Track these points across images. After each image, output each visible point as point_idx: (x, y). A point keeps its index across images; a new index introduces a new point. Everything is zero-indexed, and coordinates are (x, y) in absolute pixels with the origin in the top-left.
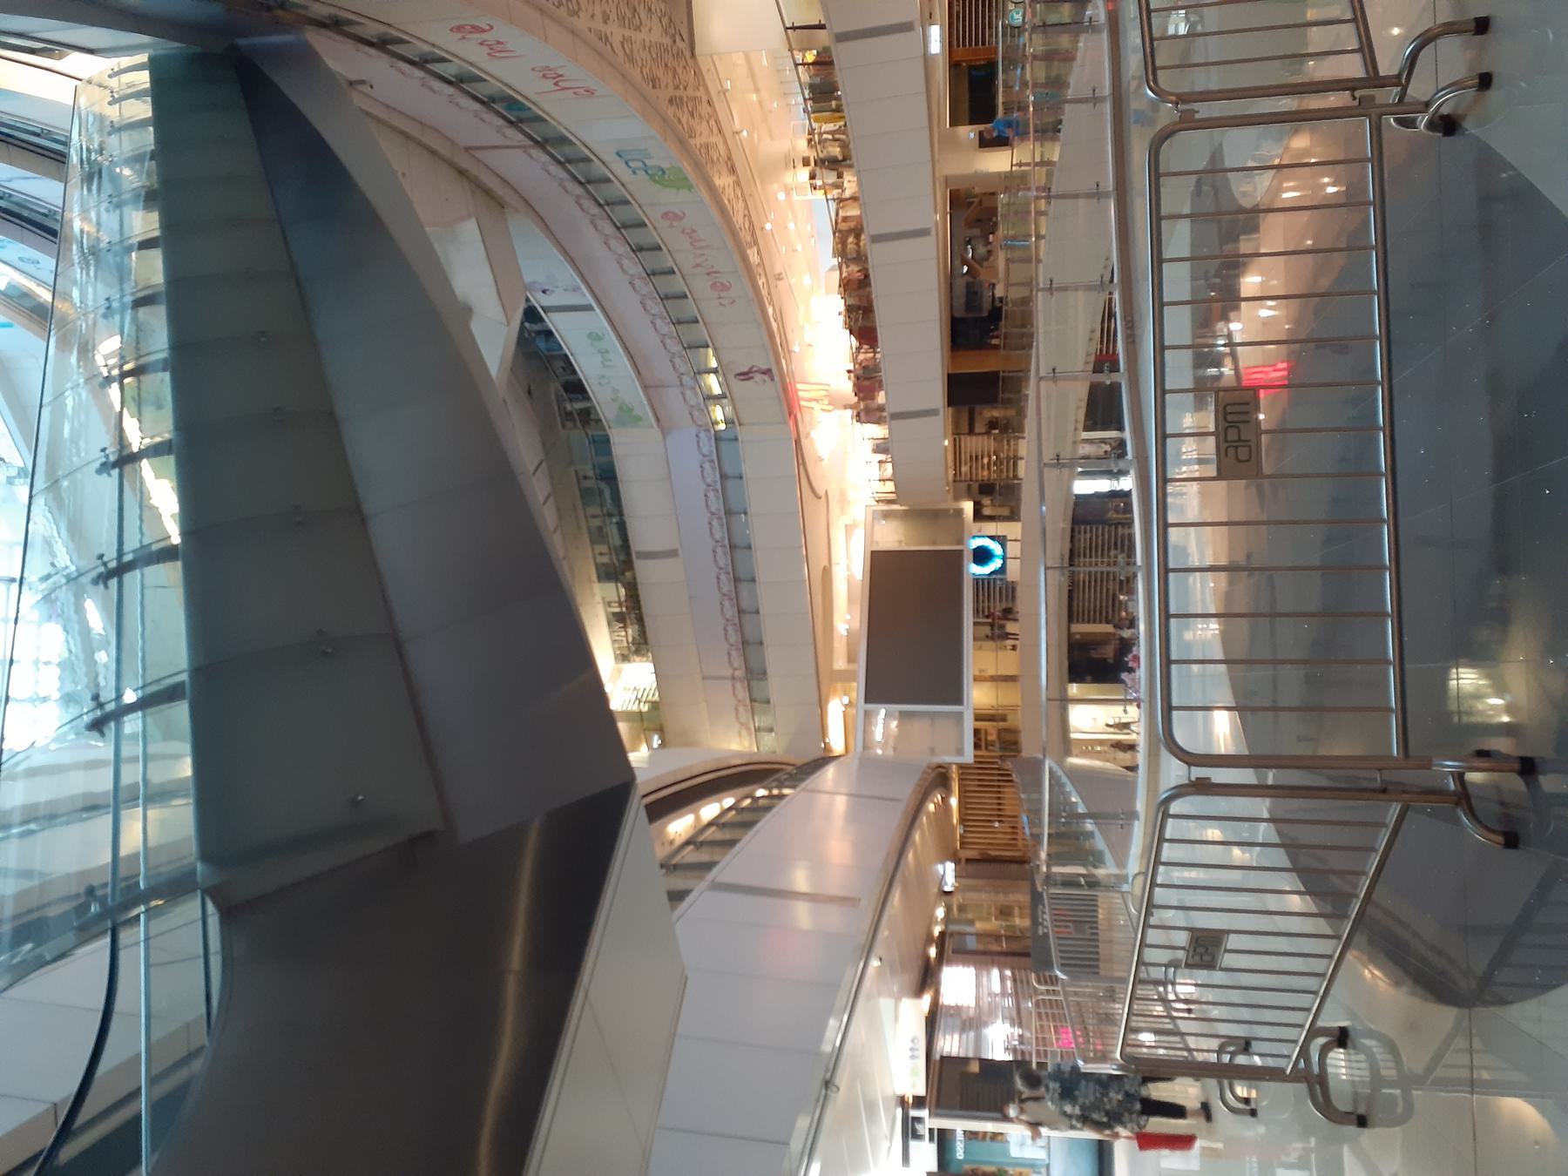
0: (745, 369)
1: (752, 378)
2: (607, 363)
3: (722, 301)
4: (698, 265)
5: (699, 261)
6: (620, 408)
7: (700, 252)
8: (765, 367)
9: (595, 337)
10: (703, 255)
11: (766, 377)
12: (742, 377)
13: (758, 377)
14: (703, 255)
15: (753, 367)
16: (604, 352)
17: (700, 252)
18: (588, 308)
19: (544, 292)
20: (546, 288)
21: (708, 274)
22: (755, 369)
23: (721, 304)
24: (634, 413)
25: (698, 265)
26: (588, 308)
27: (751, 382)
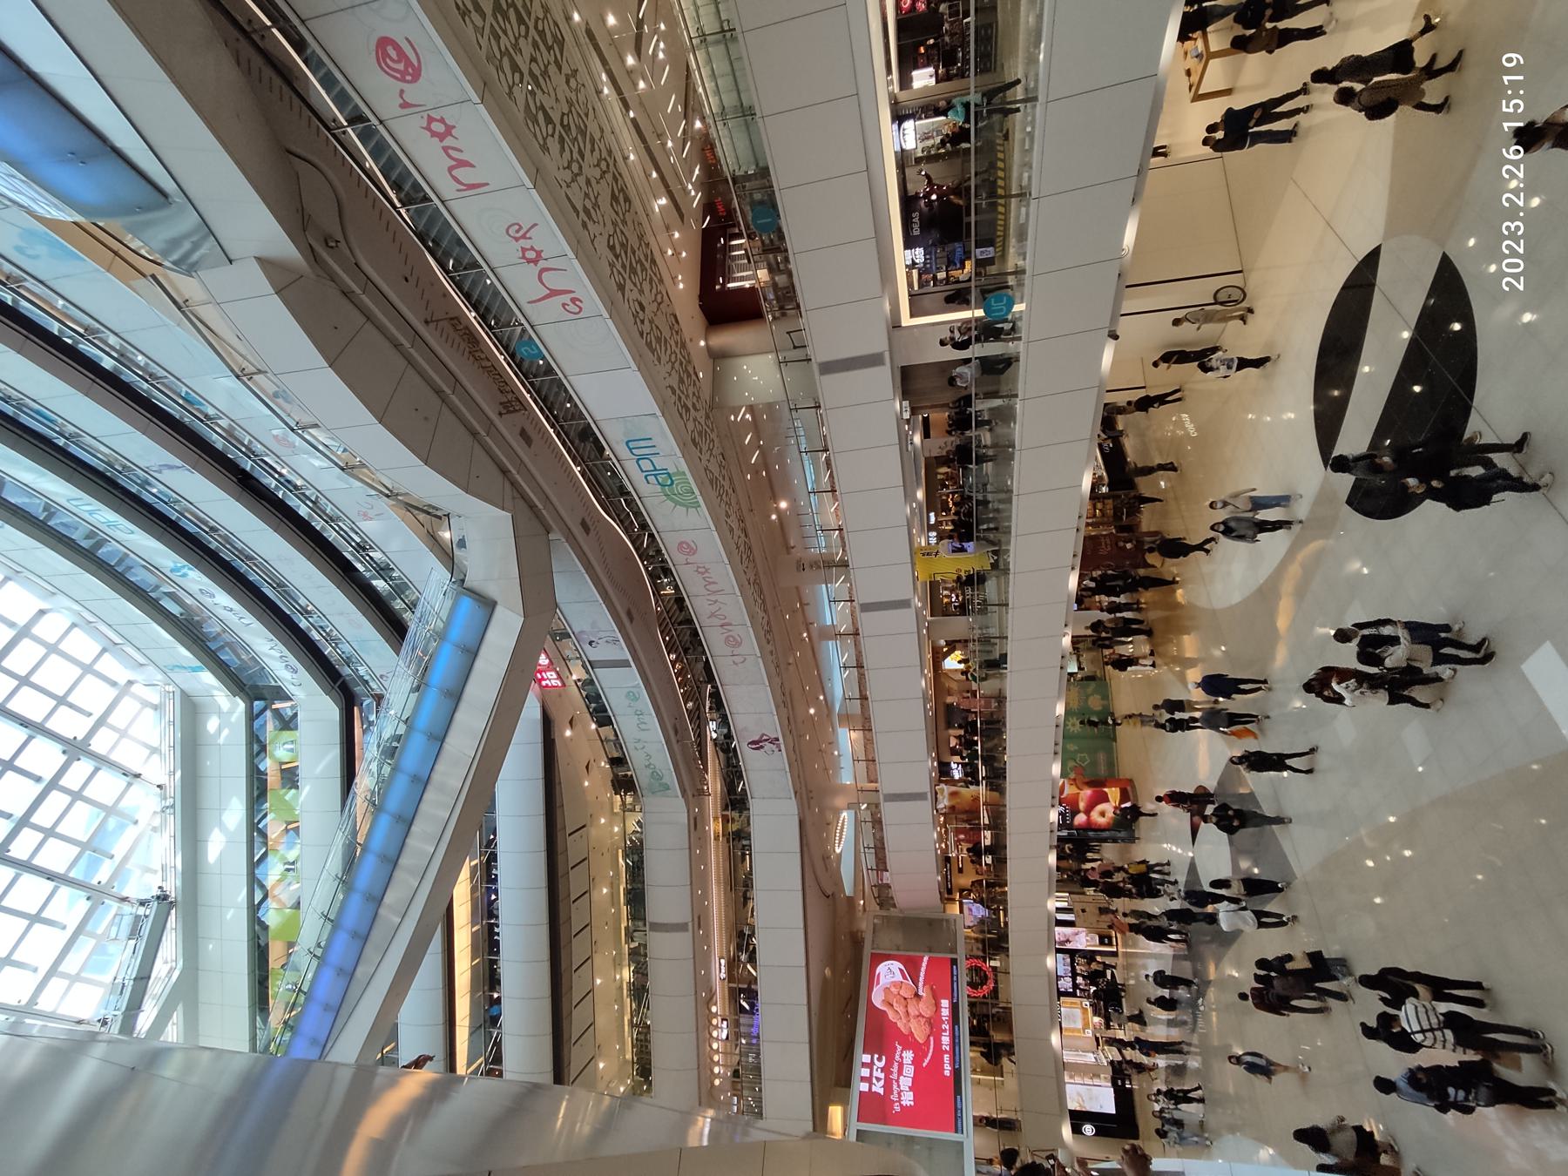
0: (756, 738)
1: (762, 747)
2: (643, 726)
4: (713, 615)
5: (714, 608)
7: (713, 598)
8: (773, 736)
10: (716, 602)
13: (768, 746)
14: (716, 602)
15: (763, 735)
17: (713, 598)
19: (591, 643)
22: (765, 737)
24: (664, 781)
26: (625, 664)
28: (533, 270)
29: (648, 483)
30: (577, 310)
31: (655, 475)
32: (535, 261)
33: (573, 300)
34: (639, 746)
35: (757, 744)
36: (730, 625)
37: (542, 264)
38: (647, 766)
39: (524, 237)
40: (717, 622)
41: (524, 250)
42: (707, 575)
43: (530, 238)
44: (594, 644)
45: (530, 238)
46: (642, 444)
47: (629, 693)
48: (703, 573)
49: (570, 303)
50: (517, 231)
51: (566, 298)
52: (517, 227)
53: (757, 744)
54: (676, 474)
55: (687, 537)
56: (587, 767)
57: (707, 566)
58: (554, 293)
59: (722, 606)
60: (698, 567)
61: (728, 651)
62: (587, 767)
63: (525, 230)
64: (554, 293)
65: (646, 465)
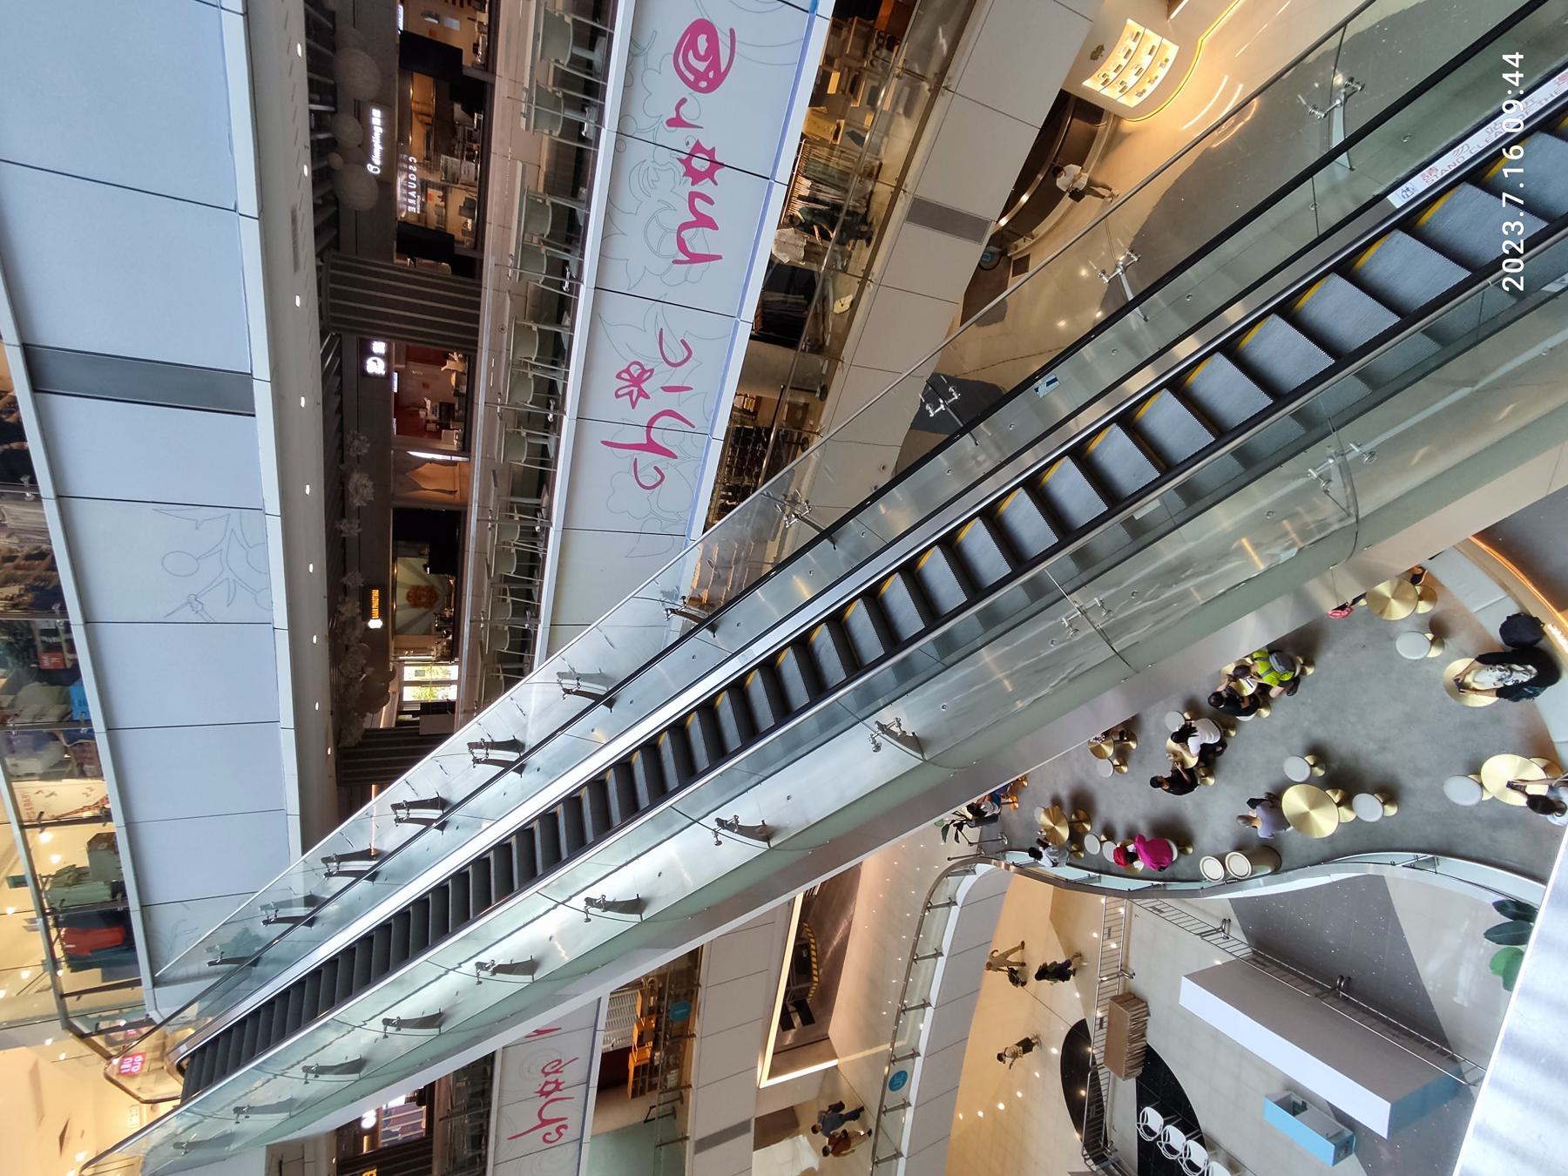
28: (544, 1100)
33: (558, 1130)
37: (555, 1095)
39: (557, 1072)
43: (562, 1072)
50: (553, 1068)
51: (552, 1128)
52: (557, 1063)
64: (545, 1123)
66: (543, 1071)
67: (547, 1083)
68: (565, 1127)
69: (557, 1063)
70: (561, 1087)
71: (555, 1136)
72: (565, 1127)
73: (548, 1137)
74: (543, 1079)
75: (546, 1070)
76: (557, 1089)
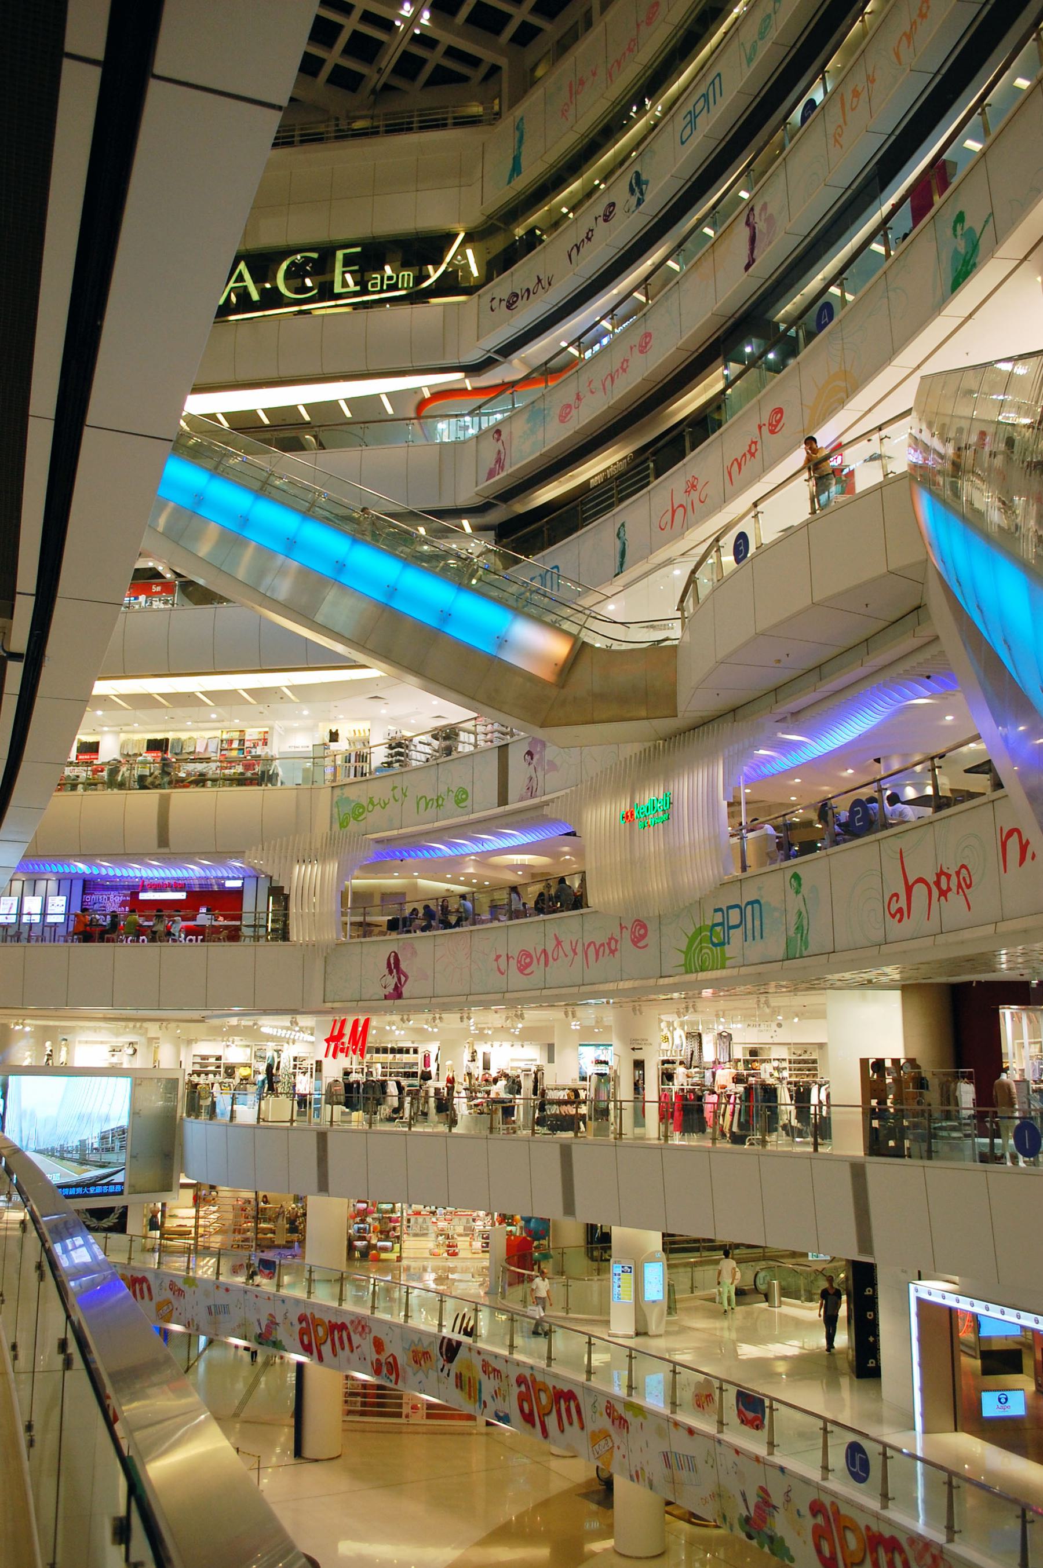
0: (403, 966)
1: (391, 972)
3: (504, 958)
4: (559, 943)
6: (359, 805)
7: (579, 949)
8: (406, 991)
9: (461, 797)
10: (575, 953)
11: (390, 989)
12: (392, 961)
13: (392, 981)
14: (575, 953)
15: (407, 977)
16: (438, 802)
17: (579, 949)
18: (503, 800)
19: (530, 753)
20: (536, 757)
21: (544, 951)
22: (403, 979)
23: (498, 957)
25: (559, 943)
26: (503, 800)
27: (387, 972)
28: (931, 879)
29: (716, 910)
30: (893, 912)
31: (722, 924)
32: (938, 883)
33: (900, 910)
34: (398, 793)
35: (394, 965)
36: (546, 964)
37: (935, 892)
38: (371, 802)
39: (959, 886)
40: (550, 945)
41: (949, 877)
42: (607, 951)
43: (958, 893)
44: (528, 758)
45: (958, 893)
46: (757, 923)
47: (466, 793)
48: (609, 944)
49: (899, 905)
51: (903, 903)
52: (968, 882)
53: (394, 965)
54: (723, 953)
55: (651, 938)
56: (376, 697)
57: (617, 954)
58: (909, 889)
59: (570, 957)
60: (617, 941)
61: (515, 953)
62: (376, 697)
63: (966, 890)
64: (909, 889)
65: (734, 917)
66: (963, 866)
67: (949, 877)
68: (900, 921)
69: (968, 882)
70: (942, 898)
71: (894, 908)
72: (900, 921)
73: (895, 898)
74: (952, 872)
75: (964, 871)
76: (943, 893)
